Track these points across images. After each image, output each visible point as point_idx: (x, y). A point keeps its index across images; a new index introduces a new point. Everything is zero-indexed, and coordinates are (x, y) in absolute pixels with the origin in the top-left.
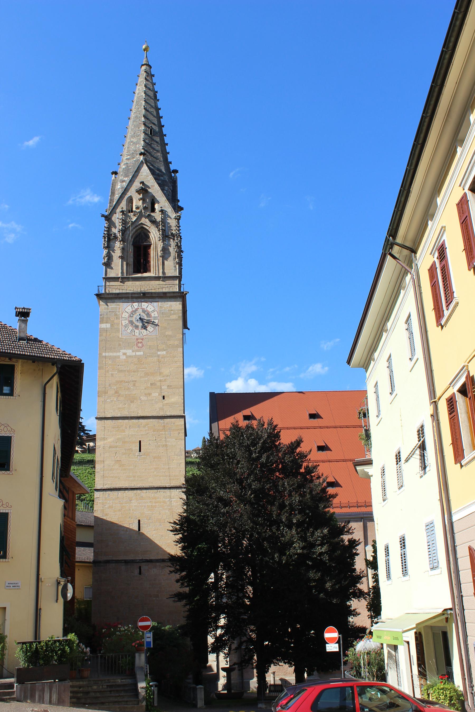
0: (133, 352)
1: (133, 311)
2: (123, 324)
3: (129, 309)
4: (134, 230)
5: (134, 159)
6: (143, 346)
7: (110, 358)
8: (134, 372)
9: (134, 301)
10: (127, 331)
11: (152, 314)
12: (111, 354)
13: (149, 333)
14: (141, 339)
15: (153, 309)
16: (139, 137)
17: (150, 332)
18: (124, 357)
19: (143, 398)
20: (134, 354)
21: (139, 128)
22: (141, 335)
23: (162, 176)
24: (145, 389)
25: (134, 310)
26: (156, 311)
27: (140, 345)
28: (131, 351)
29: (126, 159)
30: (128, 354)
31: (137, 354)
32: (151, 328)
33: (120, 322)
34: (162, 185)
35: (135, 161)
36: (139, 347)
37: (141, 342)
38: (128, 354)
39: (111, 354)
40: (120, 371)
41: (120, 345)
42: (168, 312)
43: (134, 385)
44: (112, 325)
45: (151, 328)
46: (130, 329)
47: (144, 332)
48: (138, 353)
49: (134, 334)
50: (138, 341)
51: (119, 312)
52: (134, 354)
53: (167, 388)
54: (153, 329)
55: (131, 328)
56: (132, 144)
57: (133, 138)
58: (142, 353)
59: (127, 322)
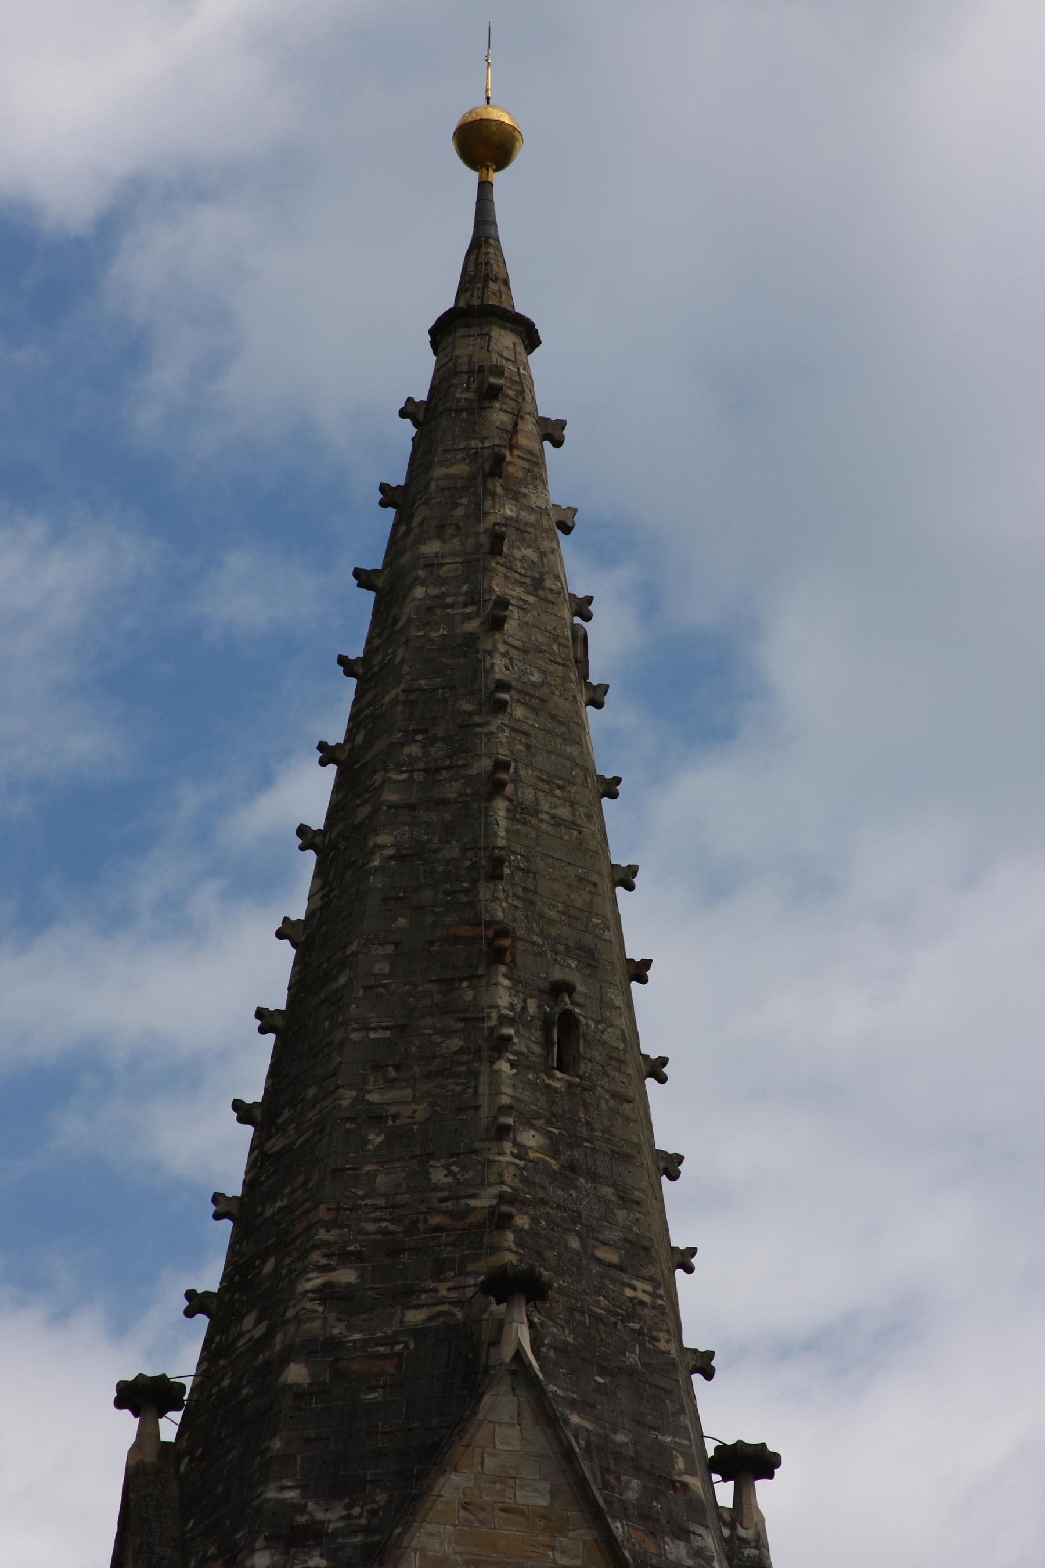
5: (415, 1317)
16: (452, 1085)
21: (448, 984)
23: (683, 1534)
29: (327, 1294)
35: (417, 1333)
56: (375, 1138)
57: (391, 1083)
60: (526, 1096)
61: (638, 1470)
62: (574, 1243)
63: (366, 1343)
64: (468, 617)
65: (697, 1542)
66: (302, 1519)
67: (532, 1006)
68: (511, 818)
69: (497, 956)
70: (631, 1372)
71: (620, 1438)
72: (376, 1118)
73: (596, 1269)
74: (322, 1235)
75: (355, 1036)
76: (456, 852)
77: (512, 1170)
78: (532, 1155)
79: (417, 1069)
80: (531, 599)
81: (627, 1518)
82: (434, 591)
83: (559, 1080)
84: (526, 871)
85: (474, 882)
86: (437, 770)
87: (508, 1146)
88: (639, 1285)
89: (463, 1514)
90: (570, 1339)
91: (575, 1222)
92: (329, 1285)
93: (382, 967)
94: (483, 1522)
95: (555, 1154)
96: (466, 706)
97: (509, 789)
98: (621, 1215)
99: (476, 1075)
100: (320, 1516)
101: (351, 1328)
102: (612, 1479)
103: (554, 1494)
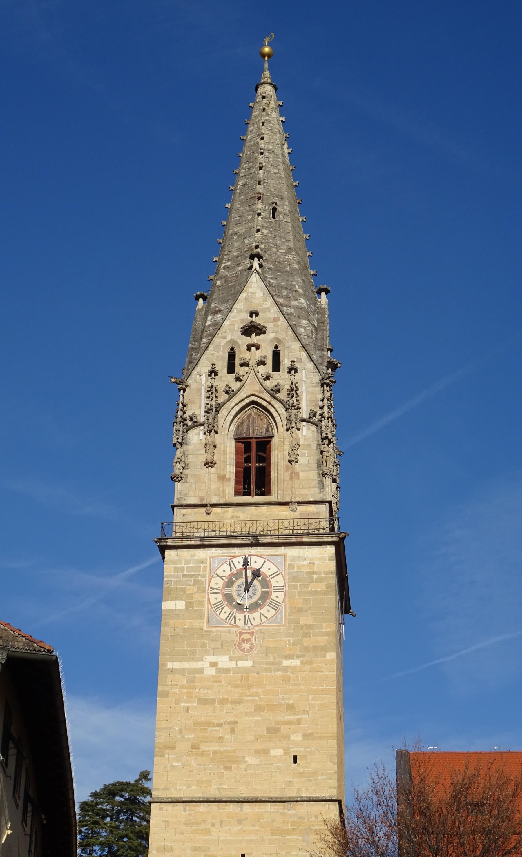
0: (231, 659)
1: (232, 575)
2: (212, 603)
3: (224, 571)
4: (237, 408)
5: (240, 268)
6: (251, 649)
7: (182, 671)
8: (233, 702)
9: (235, 553)
10: (221, 616)
11: (272, 580)
12: (186, 665)
13: (266, 619)
14: (248, 633)
15: (274, 569)
17: (267, 618)
18: (212, 672)
19: (251, 760)
20: (233, 664)
22: (249, 624)
23: (297, 300)
24: (256, 740)
25: (235, 572)
26: (281, 575)
27: (246, 646)
28: (226, 658)
29: (224, 268)
30: (220, 665)
31: (239, 665)
32: (269, 611)
33: (205, 597)
34: (295, 316)
36: (243, 650)
37: (248, 640)
38: (220, 665)
39: (186, 665)
40: (203, 701)
41: (204, 645)
42: (305, 576)
43: (233, 731)
44: (189, 605)
45: (269, 611)
46: (225, 612)
47: (254, 619)
48: (241, 664)
49: (235, 623)
50: (242, 638)
51: (204, 576)
52: (233, 664)
53: (303, 739)
54: (274, 612)
55: (227, 610)
56: (235, 237)
58: (248, 663)
59: (220, 597)
60: (265, 224)
61: (286, 289)
62: (274, 250)
63: (231, 275)
64: (257, 139)
65: (300, 301)
66: (217, 309)
67: (267, 207)
68: (264, 173)
69: (259, 199)
70: (287, 272)
71: (283, 284)
72: (236, 234)
73: (279, 254)
74: (225, 257)
75: (233, 220)
76: (253, 182)
77: (260, 237)
78: (265, 234)
79: (243, 223)
80: (271, 133)
81: (283, 298)
82: (252, 135)
83: (273, 220)
84: (267, 183)
85: (256, 187)
86: (250, 168)
87: (260, 233)
88: (290, 256)
89: (245, 300)
90: (272, 267)
91: (275, 245)
92: (226, 266)
93: (239, 206)
94: (249, 302)
95: (271, 234)
96: (256, 155)
97: (263, 168)
98: (286, 243)
99: (254, 221)
100: (221, 308)
101: (229, 273)
102: (280, 291)
103: (264, 294)
